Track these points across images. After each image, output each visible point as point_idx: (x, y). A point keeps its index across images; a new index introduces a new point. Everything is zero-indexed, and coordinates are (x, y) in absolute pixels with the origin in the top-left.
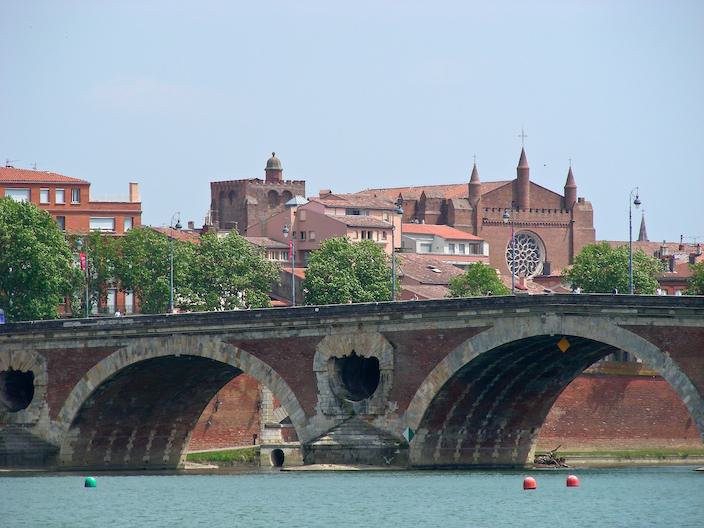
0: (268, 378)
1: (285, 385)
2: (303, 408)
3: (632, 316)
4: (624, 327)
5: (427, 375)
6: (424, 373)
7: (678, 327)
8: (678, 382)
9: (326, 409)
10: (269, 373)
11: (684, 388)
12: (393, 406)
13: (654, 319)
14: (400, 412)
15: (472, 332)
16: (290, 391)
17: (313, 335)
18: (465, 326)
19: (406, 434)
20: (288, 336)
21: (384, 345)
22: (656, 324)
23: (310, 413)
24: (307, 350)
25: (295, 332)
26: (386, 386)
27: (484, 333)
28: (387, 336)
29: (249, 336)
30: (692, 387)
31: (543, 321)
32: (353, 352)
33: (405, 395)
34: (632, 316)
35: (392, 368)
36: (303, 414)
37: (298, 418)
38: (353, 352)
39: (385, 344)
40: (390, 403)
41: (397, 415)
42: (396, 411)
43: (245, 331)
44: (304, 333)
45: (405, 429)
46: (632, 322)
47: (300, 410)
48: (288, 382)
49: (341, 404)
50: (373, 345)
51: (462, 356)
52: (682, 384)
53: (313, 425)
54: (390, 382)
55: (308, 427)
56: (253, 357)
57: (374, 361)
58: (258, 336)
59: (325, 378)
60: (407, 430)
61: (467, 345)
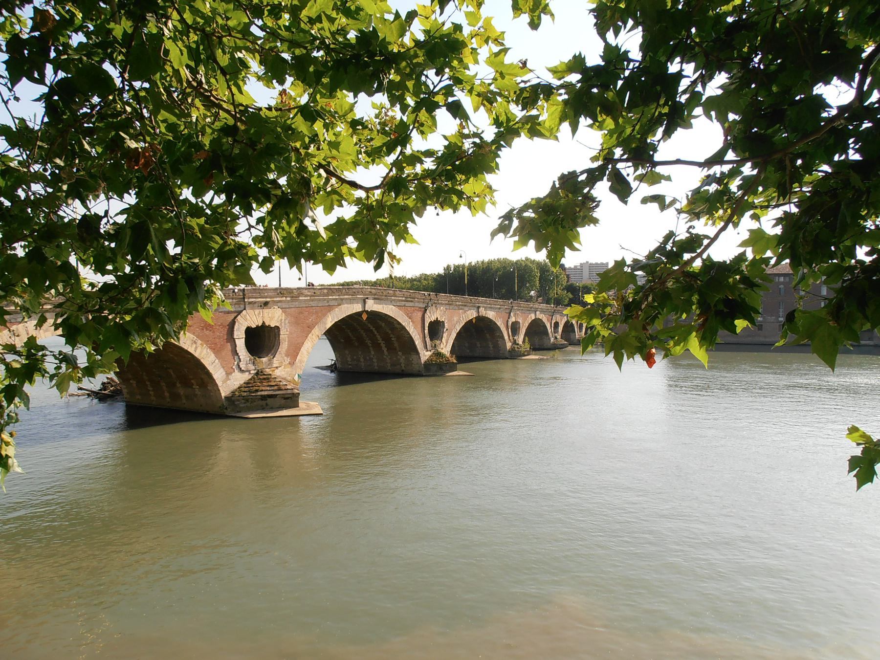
0: (194, 346)
2: (223, 367)
3: (402, 301)
5: (307, 337)
10: (195, 343)
12: (287, 360)
13: (406, 303)
14: (292, 364)
15: (330, 308)
16: (213, 355)
19: (296, 378)
21: (283, 318)
23: (228, 374)
26: (284, 346)
27: (336, 309)
32: (264, 322)
33: (294, 352)
34: (402, 301)
35: (288, 333)
36: (224, 373)
37: (220, 377)
38: (264, 322)
41: (289, 366)
42: (290, 363)
47: (222, 370)
48: (211, 348)
49: (254, 363)
50: (273, 317)
53: (232, 380)
54: (287, 343)
57: (277, 328)
59: (241, 343)
60: (297, 375)
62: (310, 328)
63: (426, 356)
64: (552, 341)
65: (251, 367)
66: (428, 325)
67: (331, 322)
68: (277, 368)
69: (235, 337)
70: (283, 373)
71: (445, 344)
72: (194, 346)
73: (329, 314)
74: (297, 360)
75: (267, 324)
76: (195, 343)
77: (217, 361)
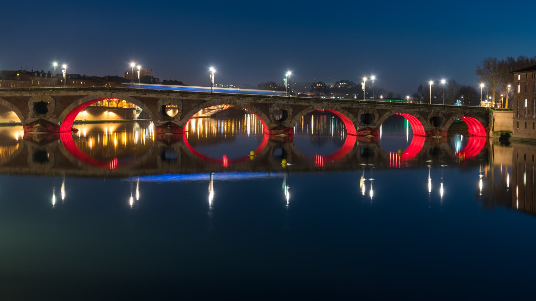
0: (12, 107)
1: (18, 109)
2: (23, 116)
4: (130, 96)
6: (65, 108)
7: (148, 97)
8: (148, 111)
9: (32, 116)
10: (12, 106)
11: (150, 113)
12: (55, 116)
16: (19, 111)
17: (28, 96)
18: (79, 95)
20: (19, 96)
22: (141, 96)
24: (26, 100)
25: (21, 95)
27: (85, 97)
28: (52, 97)
29: (5, 95)
30: (152, 113)
31: (106, 94)
32: (42, 101)
36: (24, 118)
38: (42, 101)
39: (53, 99)
40: (54, 115)
42: (56, 117)
43: (4, 94)
44: (25, 95)
45: (58, 122)
46: (133, 95)
47: (23, 116)
51: (78, 103)
52: (149, 112)
55: (26, 121)
56: (6, 102)
58: (8, 95)
59: (31, 107)
60: (59, 122)
61: (80, 100)
62: (69, 104)
63: (159, 124)
64: (358, 128)
65: (35, 116)
66: (160, 107)
67: (81, 102)
68: (49, 118)
69: (28, 105)
70: (52, 121)
71: (180, 119)
72: (12, 107)
73: (80, 99)
74: (60, 117)
75: (44, 101)
76: (12, 106)
77: (21, 113)
